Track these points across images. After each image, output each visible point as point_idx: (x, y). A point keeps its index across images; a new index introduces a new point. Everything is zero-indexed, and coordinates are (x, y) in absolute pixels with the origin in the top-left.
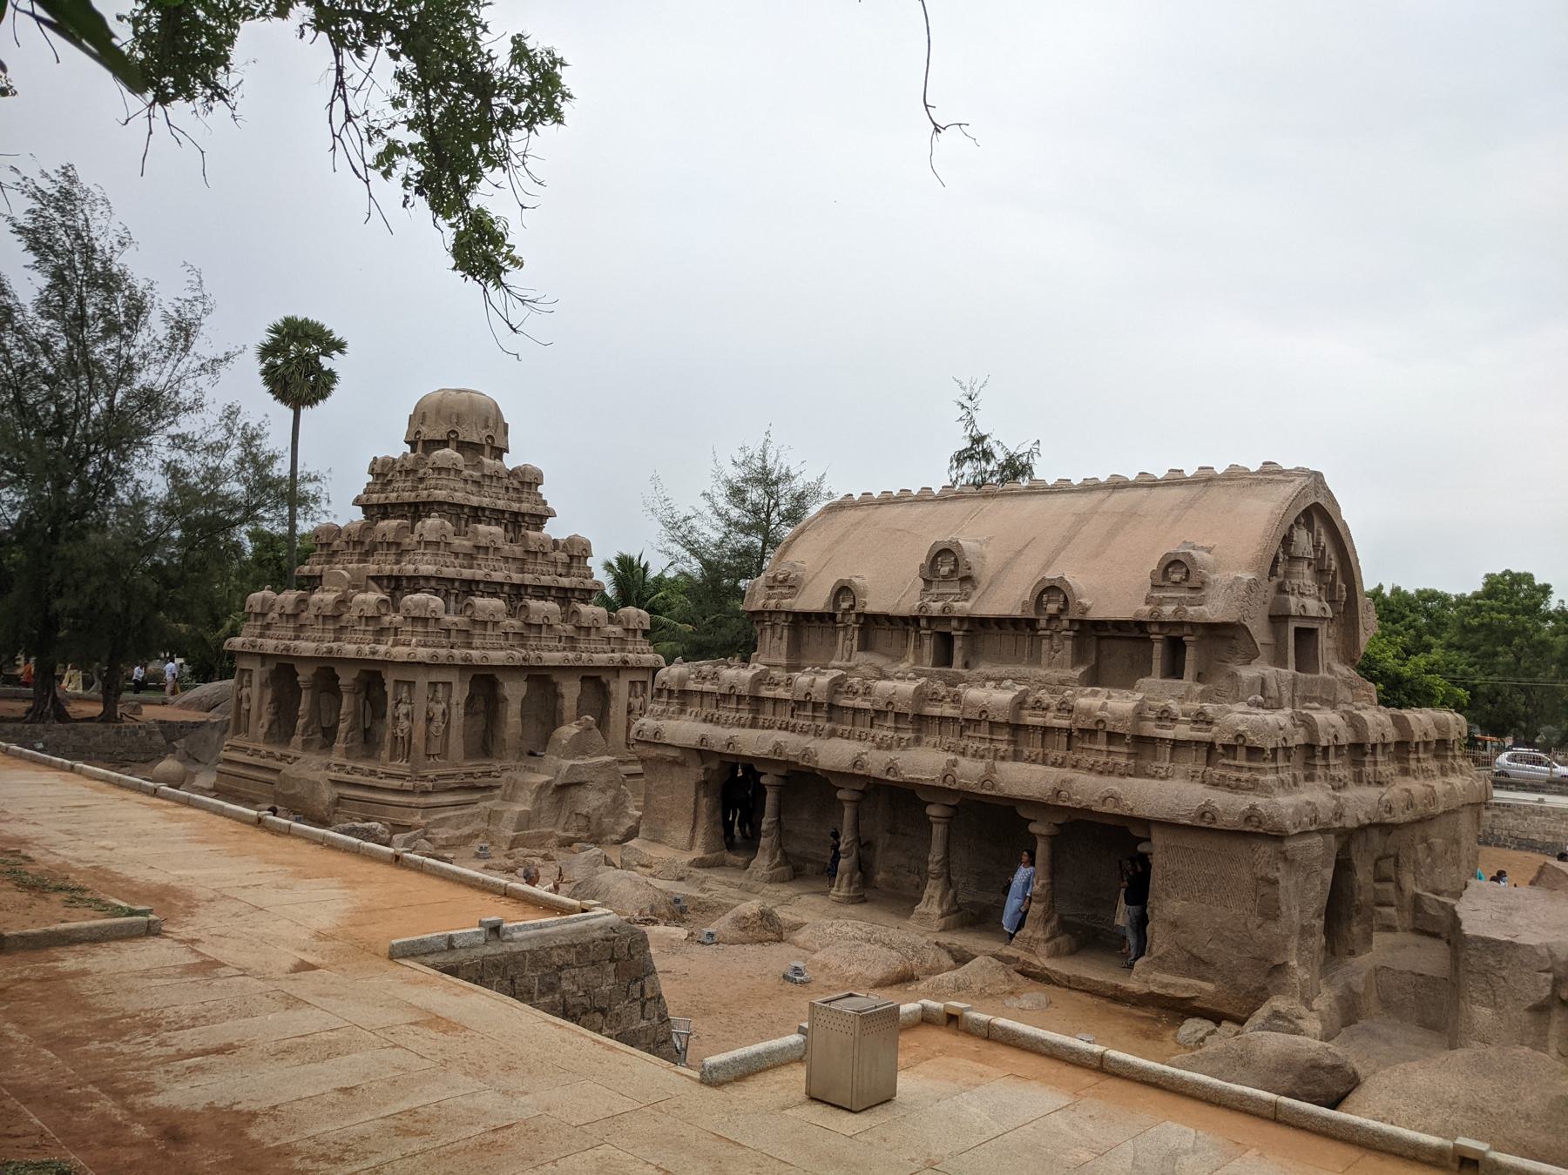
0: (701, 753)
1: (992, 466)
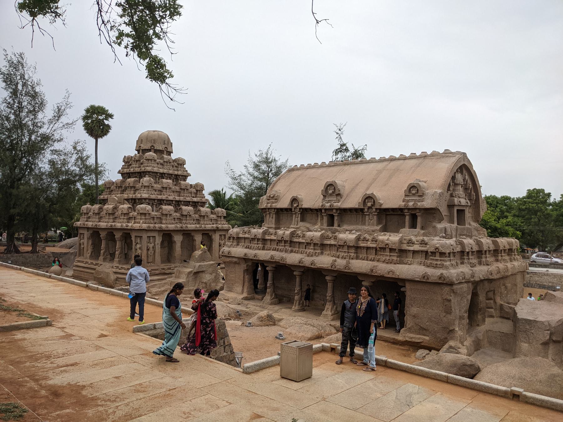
0: (245, 259)
1: (348, 154)
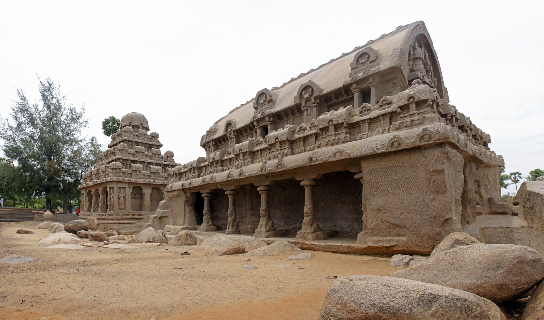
0: (184, 190)
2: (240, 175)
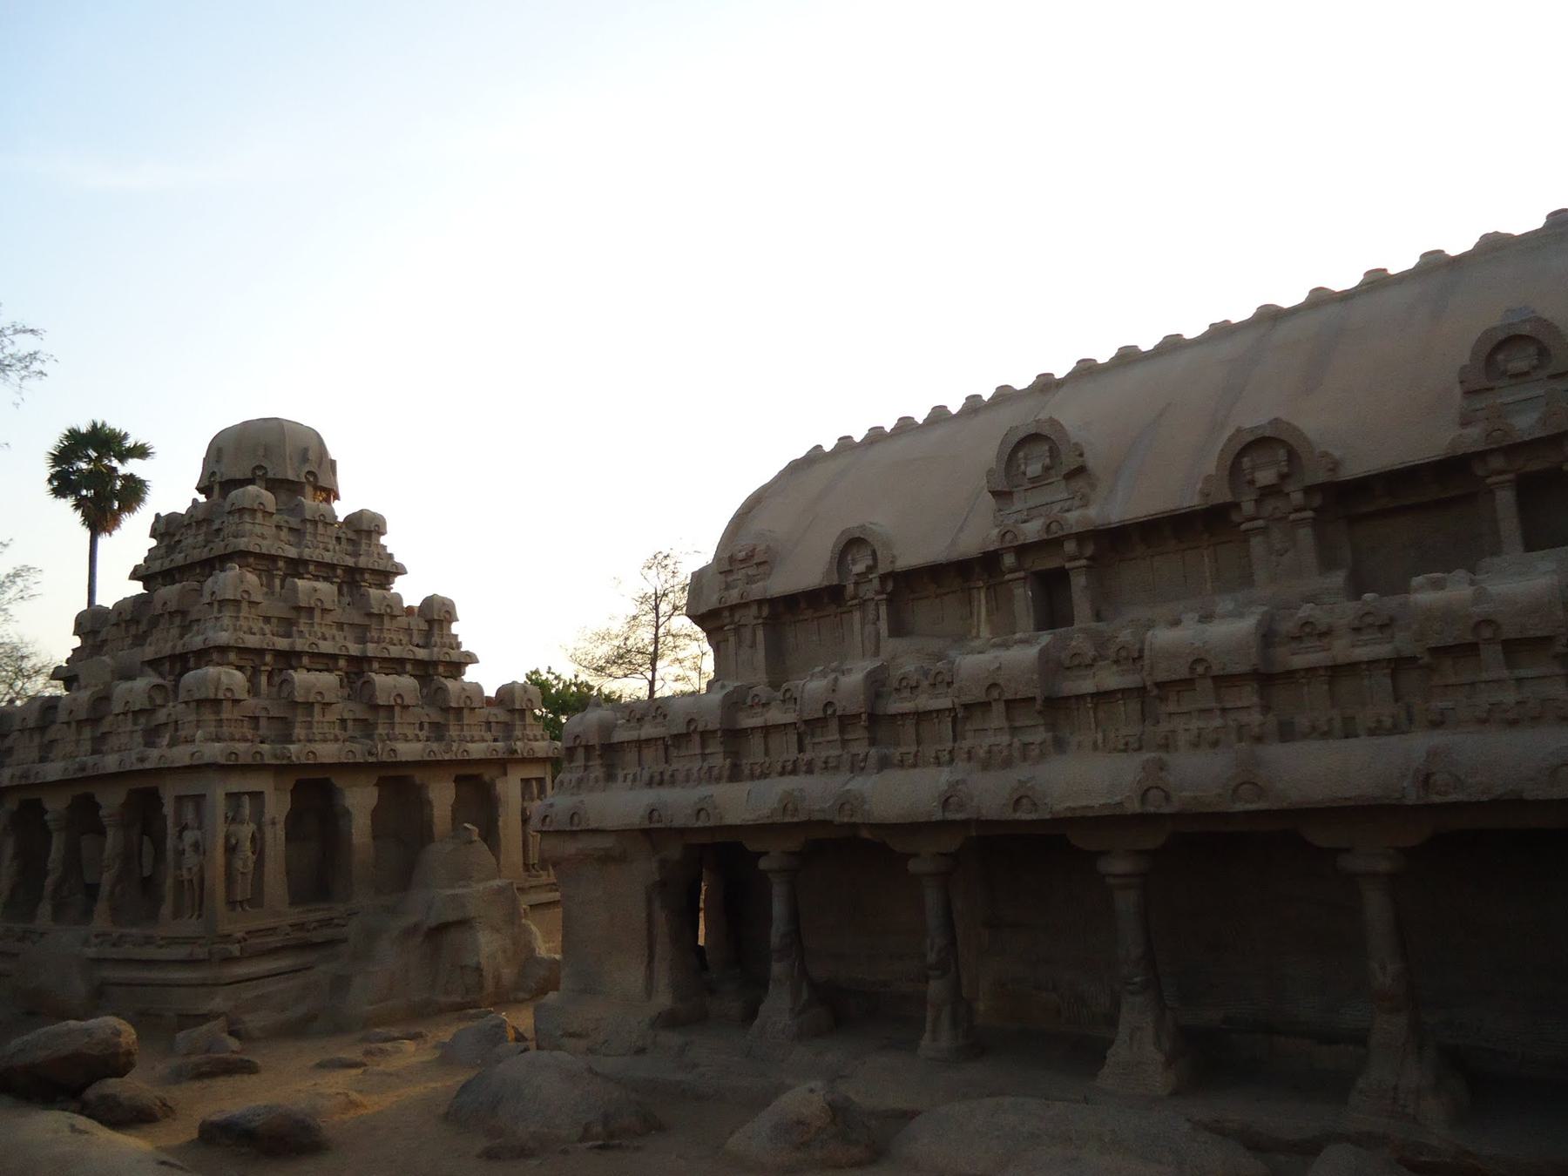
0: (652, 834)
2: (1018, 801)
